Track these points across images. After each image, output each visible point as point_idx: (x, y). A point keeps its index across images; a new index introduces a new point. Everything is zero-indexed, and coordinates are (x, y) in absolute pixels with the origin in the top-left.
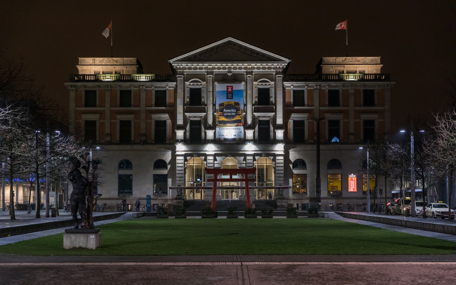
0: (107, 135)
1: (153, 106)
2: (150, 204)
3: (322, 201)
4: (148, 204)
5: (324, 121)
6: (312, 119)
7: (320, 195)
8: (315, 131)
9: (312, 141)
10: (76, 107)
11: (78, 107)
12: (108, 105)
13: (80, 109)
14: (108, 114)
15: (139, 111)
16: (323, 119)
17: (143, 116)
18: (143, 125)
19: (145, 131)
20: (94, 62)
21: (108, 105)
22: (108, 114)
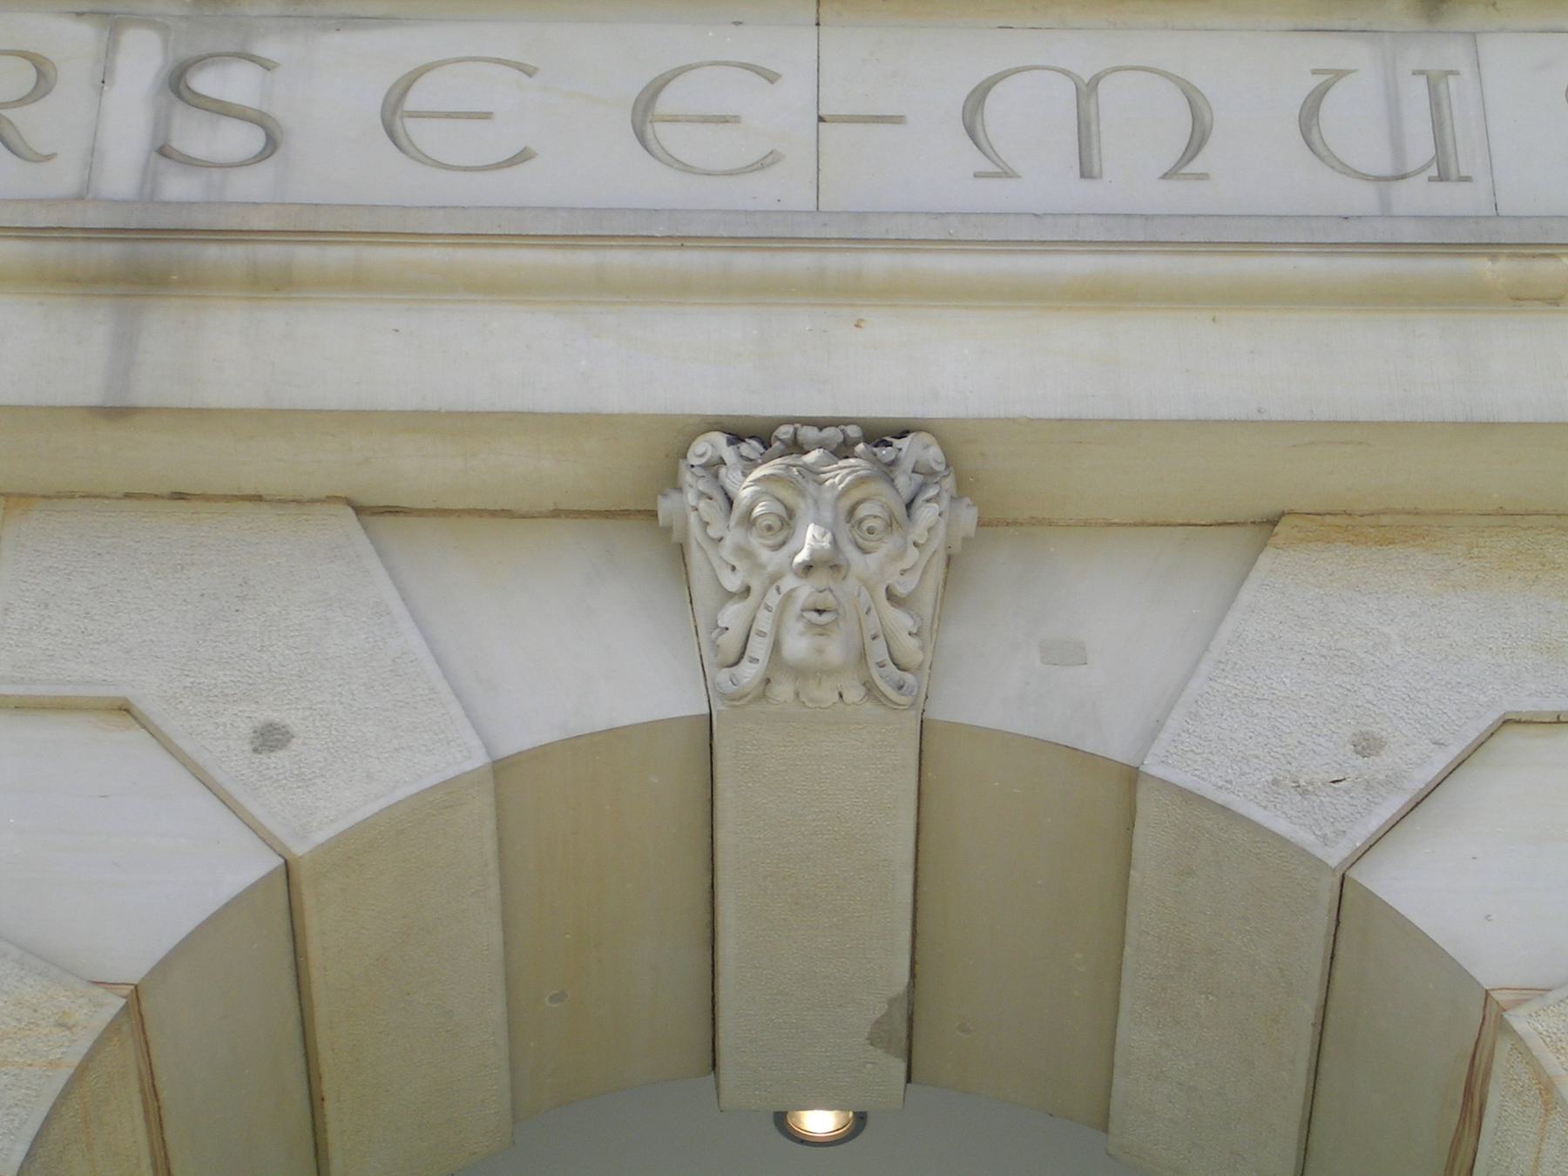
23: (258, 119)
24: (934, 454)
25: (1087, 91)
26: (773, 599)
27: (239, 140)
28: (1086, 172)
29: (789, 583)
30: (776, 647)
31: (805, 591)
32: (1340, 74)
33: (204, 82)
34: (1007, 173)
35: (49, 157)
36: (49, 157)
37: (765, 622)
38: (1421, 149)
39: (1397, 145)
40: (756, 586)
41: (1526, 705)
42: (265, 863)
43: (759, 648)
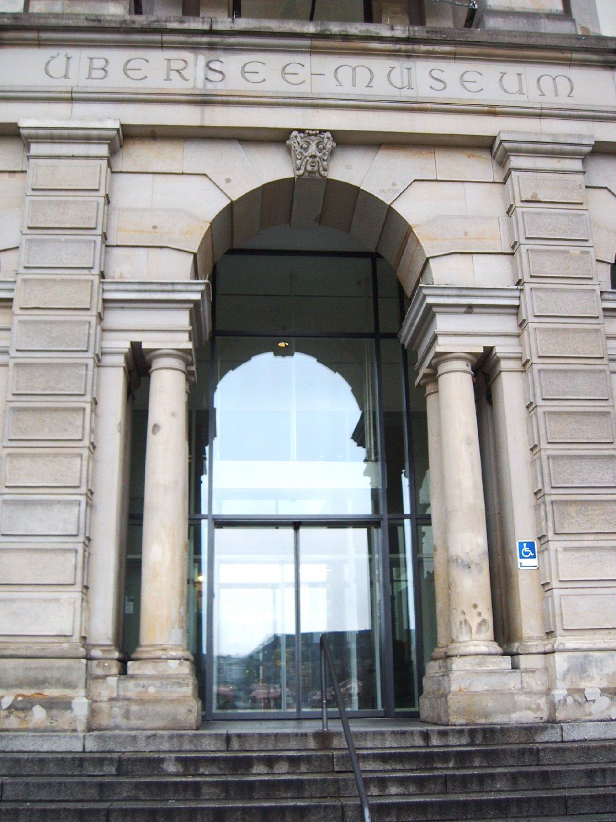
23: (221, 73)
24: (328, 135)
25: (354, 69)
26: (305, 160)
27: (218, 77)
28: (354, 85)
29: (308, 158)
30: (305, 168)
31: (310, 160)
32: (394, 68)
33: (212, 65)
34: (341, 85)
35: (188, 80)
36: (188, 80)
37: (304, 163)
38: (406, 84)
39: (402, 82)
40: (303, 158)
41: (418, 178)
42: (228, 202)
43: (303, 168)
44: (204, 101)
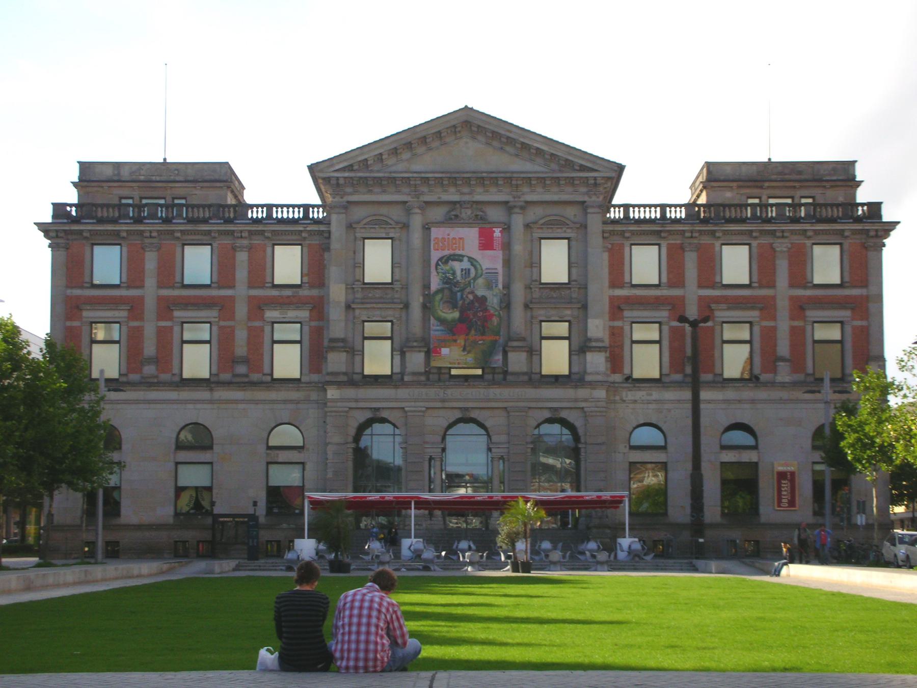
0: (149, 361)
1: (267, 285)
2: (255, 540)
3: (709, 533)
4: (251, 540)
5: (709, 324)
6: (683, 319)
7: (703, 516)
8: (689, 352)
9: (678, 377)
10: (68, 287)
11: (72, 288)
12: (150, 282)
13: (77, 292)
14: (150, 305)
15: (232, 299)
16: (705, 320)
17: (241, 310)
18: (241, 336)
19: (245, 349)
20: (116, 172)
21: (150, 282)
22: (150, 305)
44: (443, 401)
